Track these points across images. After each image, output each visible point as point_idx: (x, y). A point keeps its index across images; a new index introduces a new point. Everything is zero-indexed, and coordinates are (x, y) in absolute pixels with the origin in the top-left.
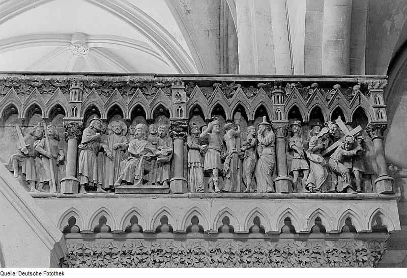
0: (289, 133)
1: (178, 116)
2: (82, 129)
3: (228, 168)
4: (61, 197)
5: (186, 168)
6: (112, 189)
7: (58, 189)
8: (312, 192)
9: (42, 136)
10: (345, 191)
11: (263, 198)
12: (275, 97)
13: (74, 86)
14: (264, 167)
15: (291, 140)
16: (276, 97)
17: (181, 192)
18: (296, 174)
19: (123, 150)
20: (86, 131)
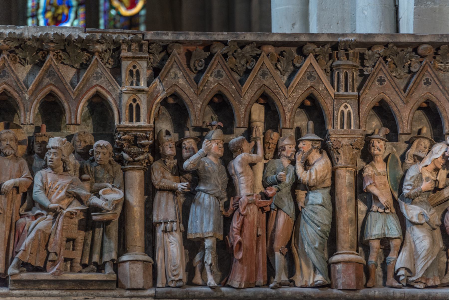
1: (131, 120)
3: (239, 238)
12: (338, 74)
15: (369, 171)
16: (342, 77)
17: (141, 286)
18: (375, 245)
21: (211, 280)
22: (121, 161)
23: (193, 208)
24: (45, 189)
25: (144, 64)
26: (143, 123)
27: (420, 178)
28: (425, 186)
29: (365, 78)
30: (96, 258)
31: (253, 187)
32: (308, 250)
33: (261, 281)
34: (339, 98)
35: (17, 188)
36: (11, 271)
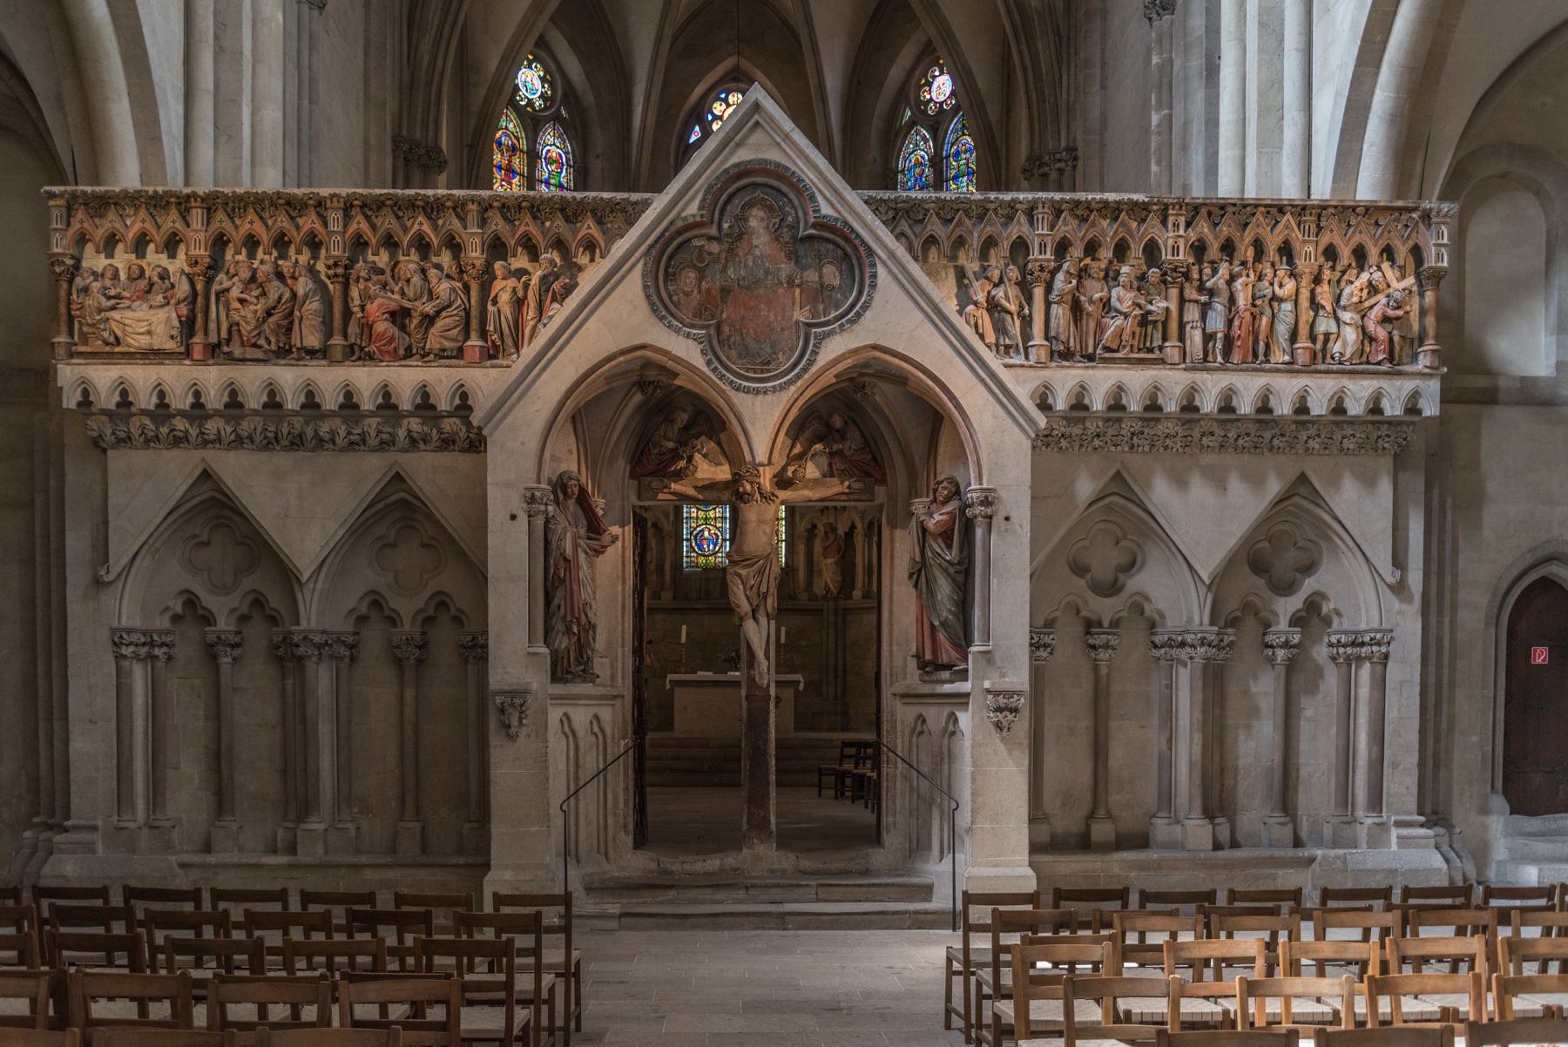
0: (1317, 280)
2: (1054, 272)
4: (1031, 367)
5: (1182, 326)
6: (1091, 358)
7: (1027, 358)
8: (1340, 363)
9: (1001, 281)
10: (1379, 363)
11: (1278, 371)
13: (1040, 210)
14: (1282, 330)
15: (1319, 290)
18: (1321, 338)
19: (1106, 304)
20: (1060, 276)
21: (1219, 359)
22: (1165, 282)
23: (1210, 312)
24: (1119, 300)
25: (1183, 218)
26: (1181, 257)
27: (1352, 295)
28: (1355, 299)
29: (1320, 229)
30: (1148, 344)
31: (1246, 300)
32: (1281, 340)
33: (1250, 359)
34: (1304, 242)
35: (1101, 299)
36: (1098, 351)
